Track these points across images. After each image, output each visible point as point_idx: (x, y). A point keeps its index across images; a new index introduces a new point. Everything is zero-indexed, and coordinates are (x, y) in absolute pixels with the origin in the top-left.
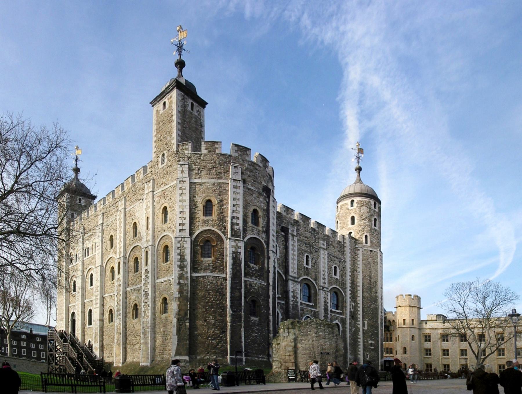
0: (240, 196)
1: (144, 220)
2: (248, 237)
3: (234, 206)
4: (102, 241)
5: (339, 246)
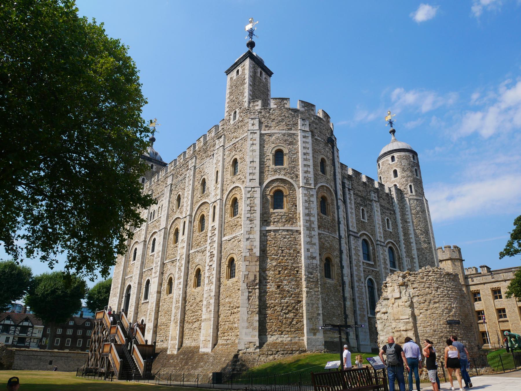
0: (310, 146)
1: (213, 175)
2: (319, 185)
3: (305, 154)
4: (169, 201)
5: (387, 198)
